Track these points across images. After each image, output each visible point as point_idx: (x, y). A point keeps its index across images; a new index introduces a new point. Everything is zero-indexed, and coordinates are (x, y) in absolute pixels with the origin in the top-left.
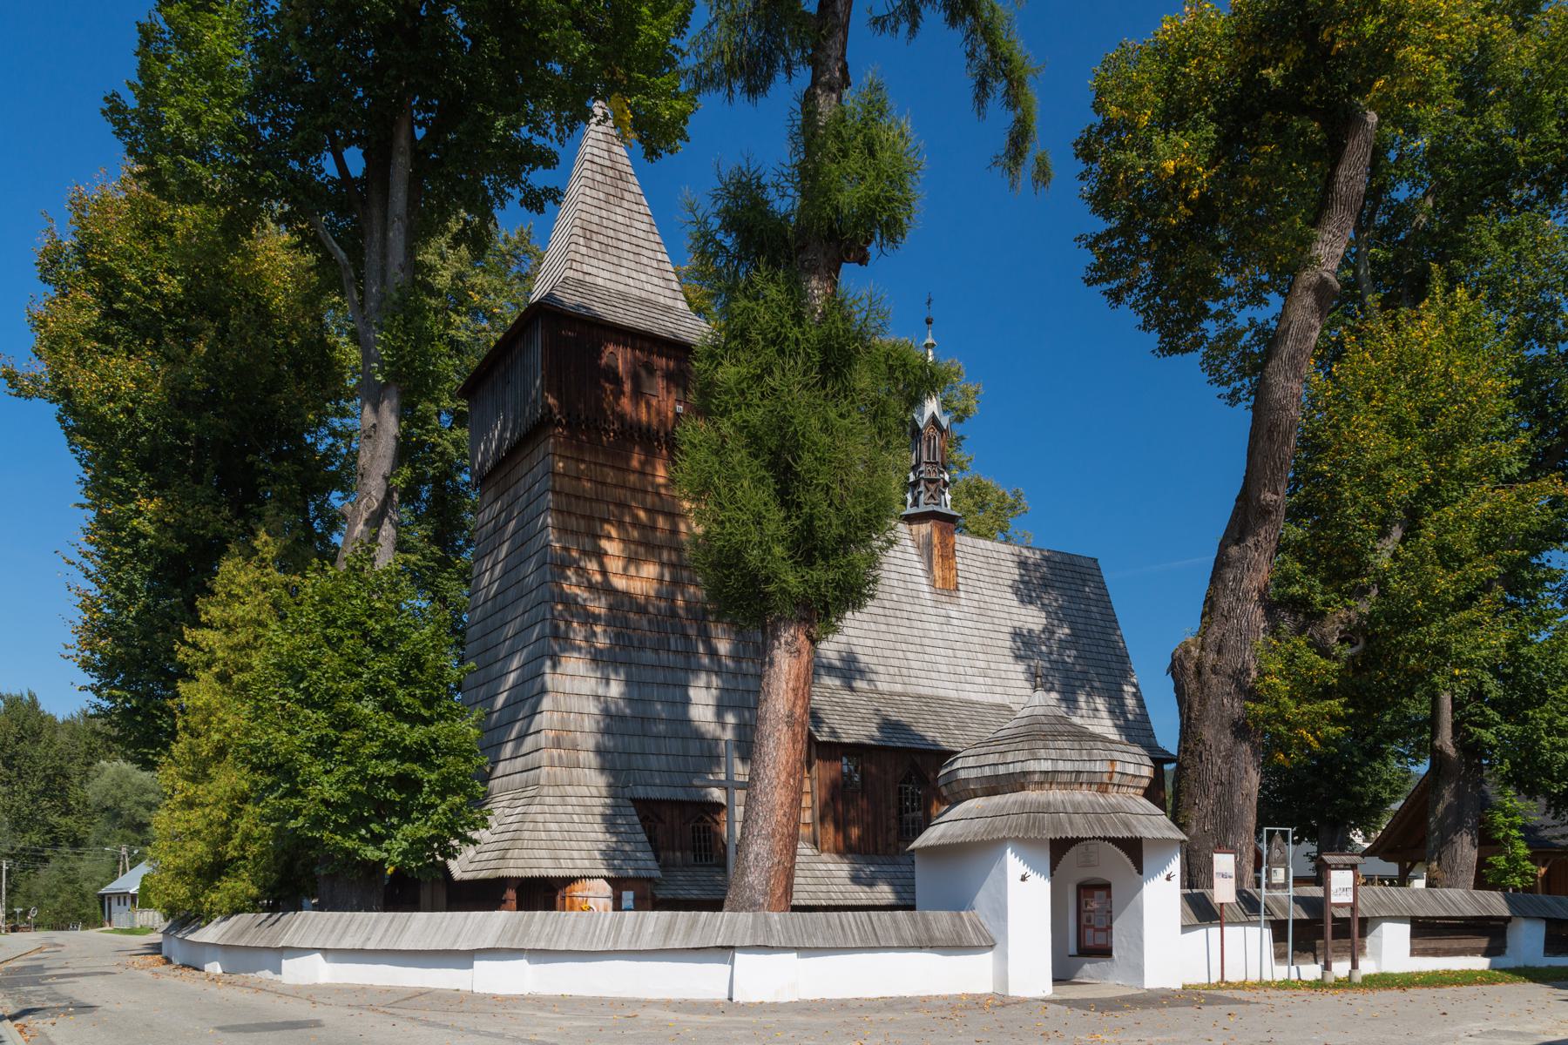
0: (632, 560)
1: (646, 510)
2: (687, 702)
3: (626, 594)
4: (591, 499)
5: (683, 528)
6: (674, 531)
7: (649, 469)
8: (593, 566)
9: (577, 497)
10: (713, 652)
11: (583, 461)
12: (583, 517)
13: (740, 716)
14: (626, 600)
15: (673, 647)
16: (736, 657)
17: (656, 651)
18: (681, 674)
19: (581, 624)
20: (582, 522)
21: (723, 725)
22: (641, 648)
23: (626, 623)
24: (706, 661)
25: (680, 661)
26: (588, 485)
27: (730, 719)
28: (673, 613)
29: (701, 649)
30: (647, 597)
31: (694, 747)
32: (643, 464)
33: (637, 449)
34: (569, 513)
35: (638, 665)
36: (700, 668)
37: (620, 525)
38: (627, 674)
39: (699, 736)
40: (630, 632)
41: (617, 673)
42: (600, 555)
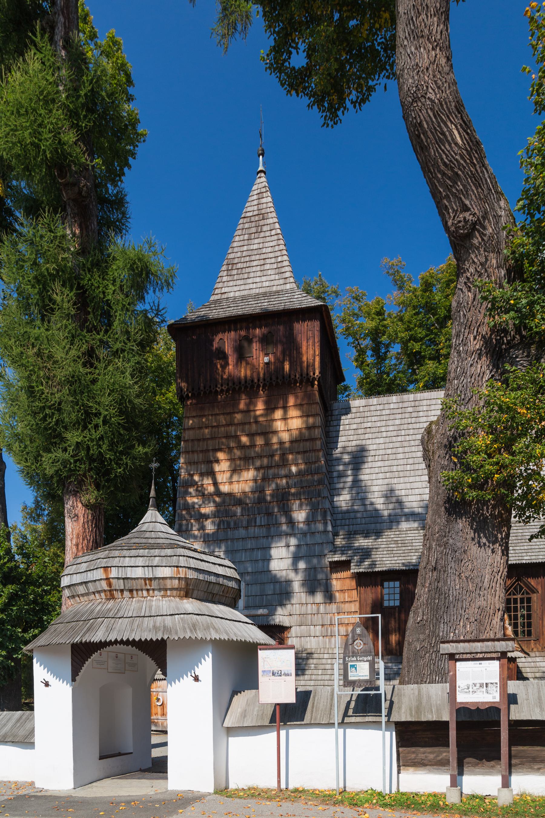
0: (235, 470)
1: (247, 435)
2: (268, 559)
3: (230, 495)
4: (208, 439)
5: (275, 440)
6: (268, 444)
7: (252, 408)
8: (207, 482)
9: (199, 440)
10: (291, 522)
11: (204, 416)
12: (202, 451)
13: (307, 563)
14: (227, 499)
15: (258, 523)
16: (308, 522)
17: (246, 528)
18: (265, 540)
19: (197, 520)
20: (201, 455)
21: (296, 570)
22: (236, 527)
23: (227, 513)
24: (284, 527)
25: (263, 531)
26: (206, 431)
27: (302, 565)
28: (261, 500)
29: (283, 520)
30: (244, 493)
31: (269, 589)
32: (248, 405)
33: (244, 397)
34: (193, 452)
35: (232, 540)
36: (280, 535)
37: (230, 450)
38: (227, 547)
39: (274, 580)
40: (228, 519)
41: (220, 548)
42: (212, 474)
